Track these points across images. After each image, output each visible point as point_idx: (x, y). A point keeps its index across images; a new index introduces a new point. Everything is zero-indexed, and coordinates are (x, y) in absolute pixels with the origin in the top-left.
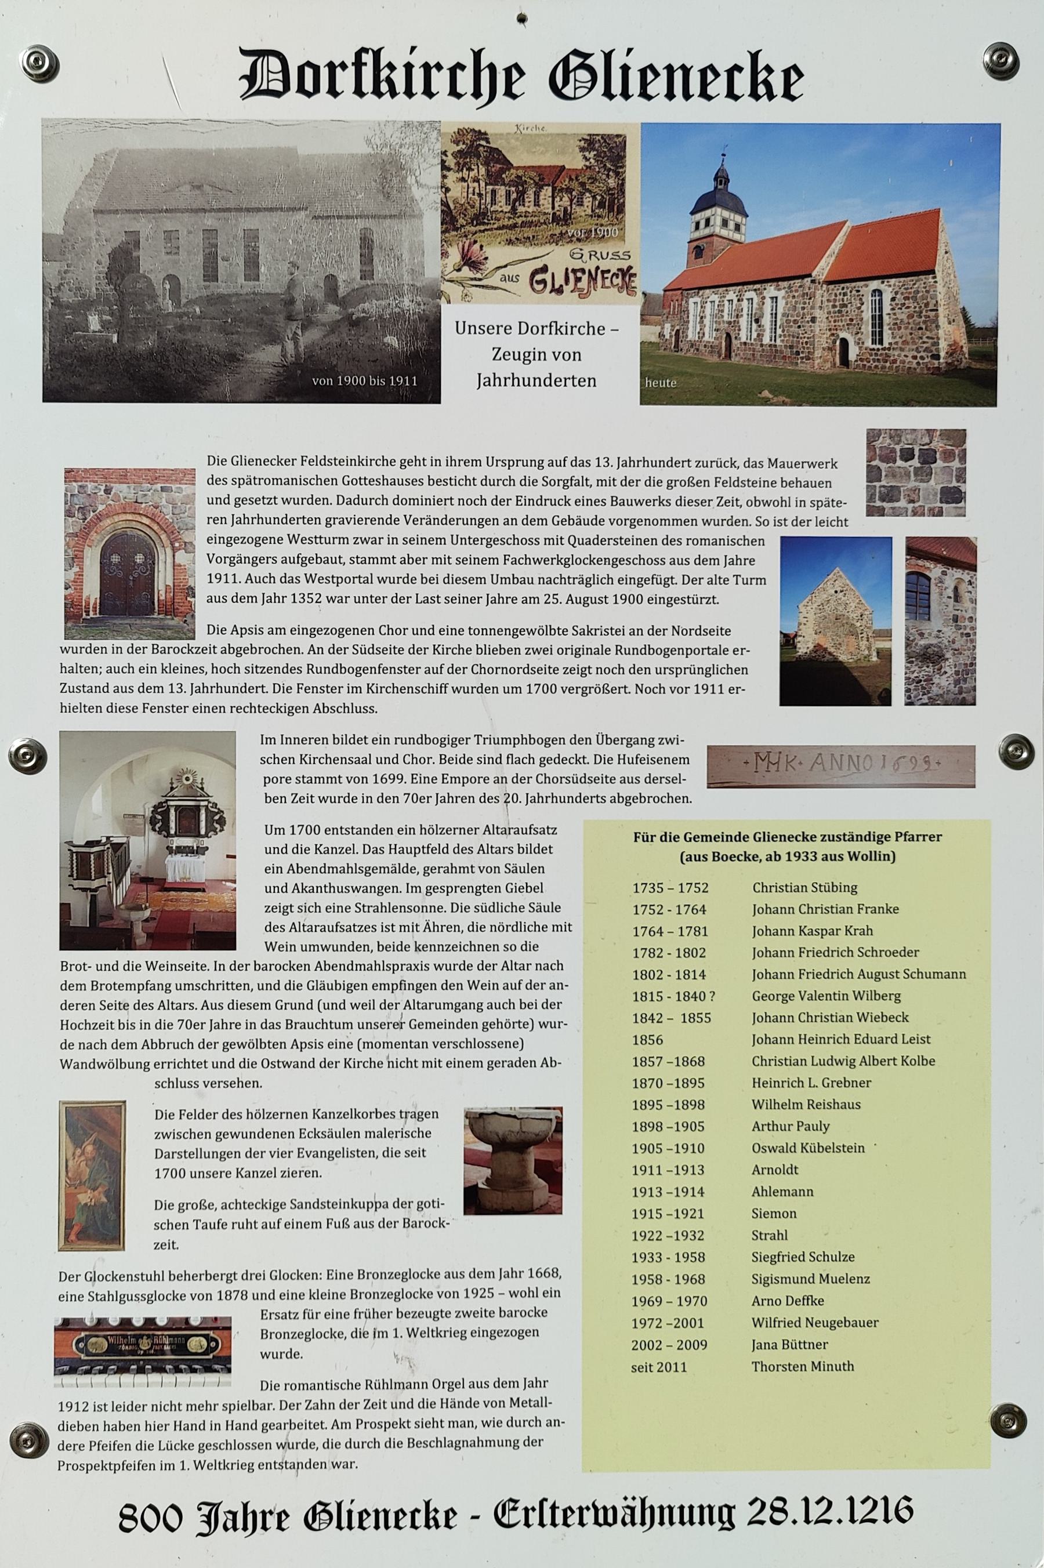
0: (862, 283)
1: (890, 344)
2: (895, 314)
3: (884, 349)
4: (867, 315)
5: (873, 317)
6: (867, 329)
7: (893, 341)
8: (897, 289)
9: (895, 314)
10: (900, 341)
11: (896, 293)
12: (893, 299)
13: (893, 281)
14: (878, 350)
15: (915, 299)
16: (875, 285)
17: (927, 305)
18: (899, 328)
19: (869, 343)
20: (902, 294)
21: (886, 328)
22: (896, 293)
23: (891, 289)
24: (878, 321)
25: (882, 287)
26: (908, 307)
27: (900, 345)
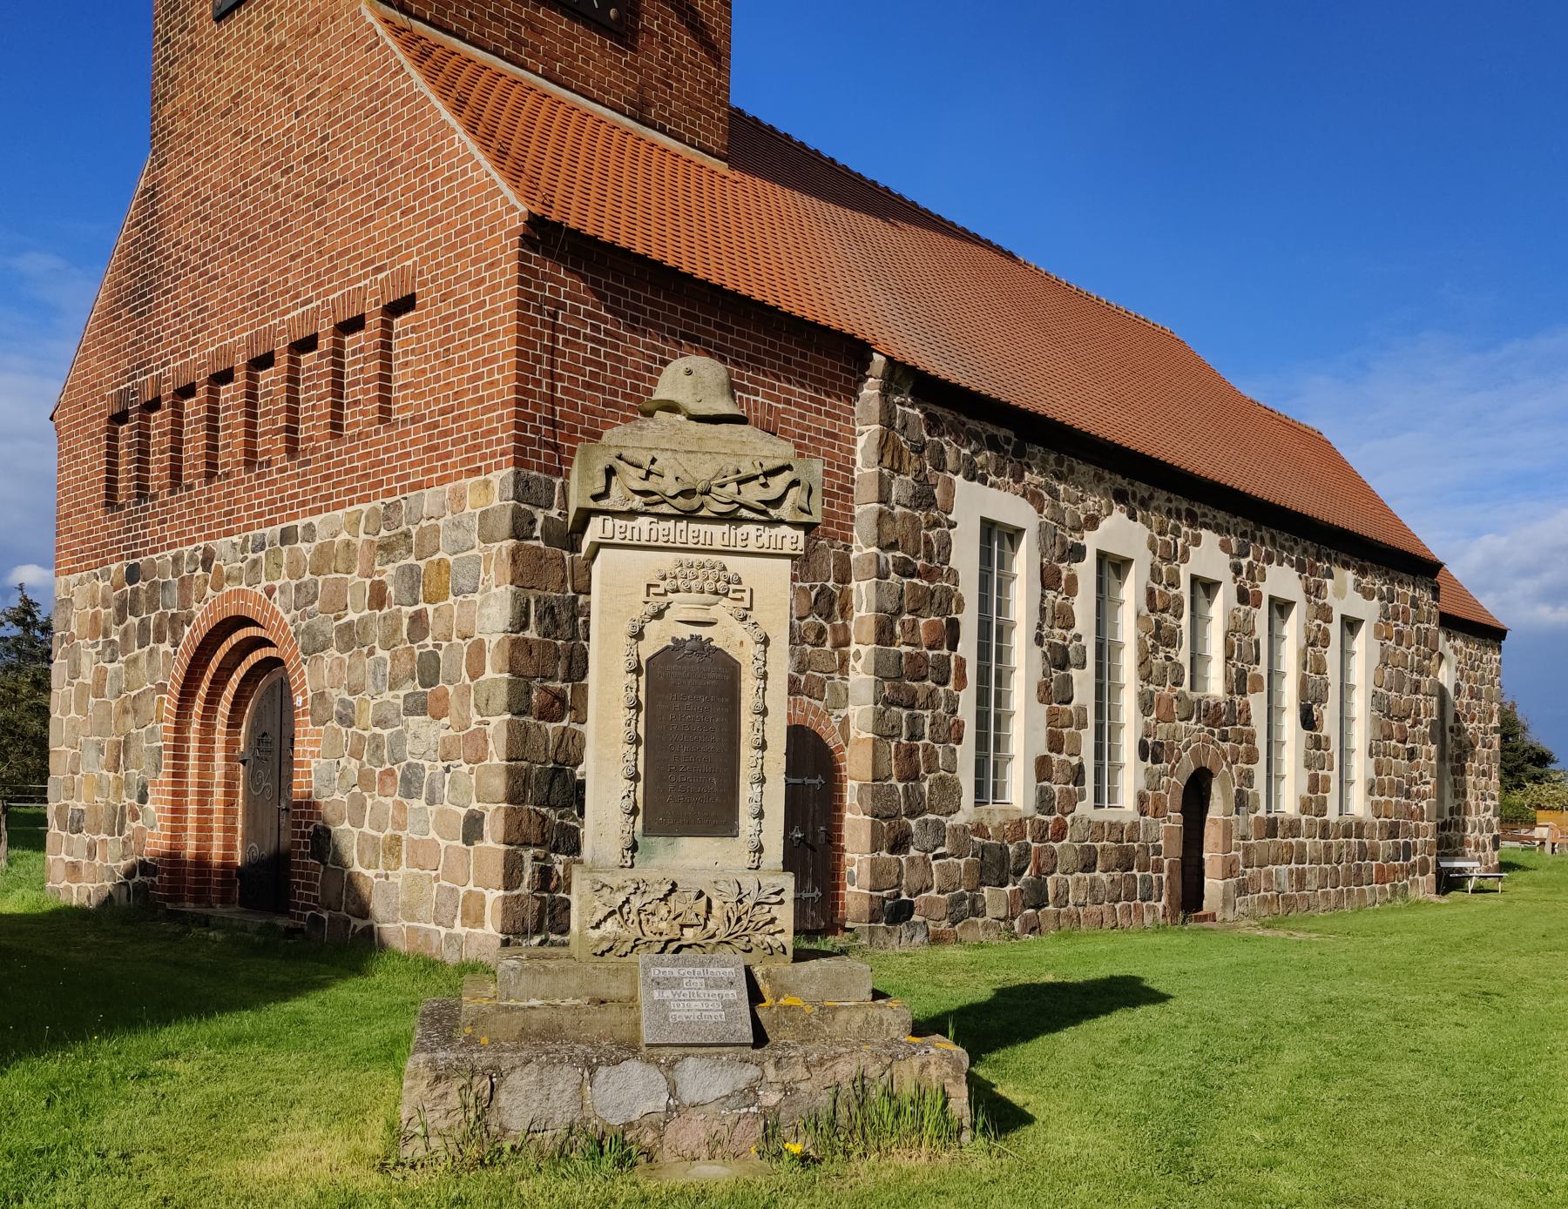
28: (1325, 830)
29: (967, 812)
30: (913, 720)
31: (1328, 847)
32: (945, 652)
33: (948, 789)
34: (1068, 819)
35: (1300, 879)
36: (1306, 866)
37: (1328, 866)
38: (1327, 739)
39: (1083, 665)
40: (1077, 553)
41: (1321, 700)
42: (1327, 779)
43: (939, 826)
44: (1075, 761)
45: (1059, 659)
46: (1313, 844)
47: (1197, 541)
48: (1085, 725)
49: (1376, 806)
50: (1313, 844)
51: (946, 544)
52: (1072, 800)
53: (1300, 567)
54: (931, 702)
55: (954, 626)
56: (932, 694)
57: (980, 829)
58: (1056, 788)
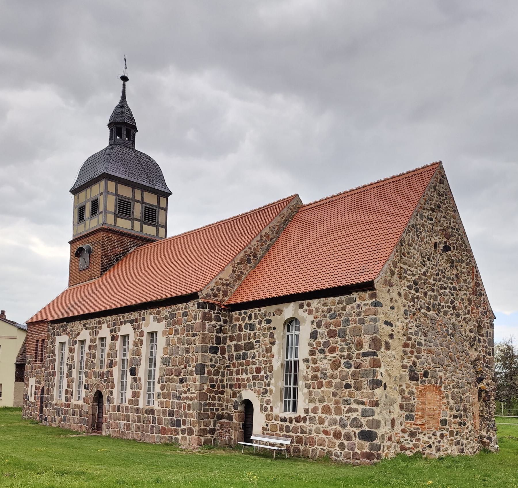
0: (272, 308)
3: (298, 420)
4: (277, 363)
6: (277, 384)
7: (311, 406)
9: (315, 362)
11: (319, 325)
12: (314, 336)
13: (315, 303)
15: (342, 334)
16: (289, 310)
17: (359, 345)
18: (320, 386)
20: (328, 325)
21: (301, 383)
22: (319, 325)
23: (311, 318)
26: (333, 350)
28: (137, 411)
31: (139, 417)
35: (127, 427)
37: (139, 424)
38: (140, 379)
39: (74, 368)
41: (138, 364)
42: (139, 393)
45: (71, 367)
46: (133, 415)
47: (101, 328)
49: (161, 404)
50: (133, 415)
53: (132, 321)
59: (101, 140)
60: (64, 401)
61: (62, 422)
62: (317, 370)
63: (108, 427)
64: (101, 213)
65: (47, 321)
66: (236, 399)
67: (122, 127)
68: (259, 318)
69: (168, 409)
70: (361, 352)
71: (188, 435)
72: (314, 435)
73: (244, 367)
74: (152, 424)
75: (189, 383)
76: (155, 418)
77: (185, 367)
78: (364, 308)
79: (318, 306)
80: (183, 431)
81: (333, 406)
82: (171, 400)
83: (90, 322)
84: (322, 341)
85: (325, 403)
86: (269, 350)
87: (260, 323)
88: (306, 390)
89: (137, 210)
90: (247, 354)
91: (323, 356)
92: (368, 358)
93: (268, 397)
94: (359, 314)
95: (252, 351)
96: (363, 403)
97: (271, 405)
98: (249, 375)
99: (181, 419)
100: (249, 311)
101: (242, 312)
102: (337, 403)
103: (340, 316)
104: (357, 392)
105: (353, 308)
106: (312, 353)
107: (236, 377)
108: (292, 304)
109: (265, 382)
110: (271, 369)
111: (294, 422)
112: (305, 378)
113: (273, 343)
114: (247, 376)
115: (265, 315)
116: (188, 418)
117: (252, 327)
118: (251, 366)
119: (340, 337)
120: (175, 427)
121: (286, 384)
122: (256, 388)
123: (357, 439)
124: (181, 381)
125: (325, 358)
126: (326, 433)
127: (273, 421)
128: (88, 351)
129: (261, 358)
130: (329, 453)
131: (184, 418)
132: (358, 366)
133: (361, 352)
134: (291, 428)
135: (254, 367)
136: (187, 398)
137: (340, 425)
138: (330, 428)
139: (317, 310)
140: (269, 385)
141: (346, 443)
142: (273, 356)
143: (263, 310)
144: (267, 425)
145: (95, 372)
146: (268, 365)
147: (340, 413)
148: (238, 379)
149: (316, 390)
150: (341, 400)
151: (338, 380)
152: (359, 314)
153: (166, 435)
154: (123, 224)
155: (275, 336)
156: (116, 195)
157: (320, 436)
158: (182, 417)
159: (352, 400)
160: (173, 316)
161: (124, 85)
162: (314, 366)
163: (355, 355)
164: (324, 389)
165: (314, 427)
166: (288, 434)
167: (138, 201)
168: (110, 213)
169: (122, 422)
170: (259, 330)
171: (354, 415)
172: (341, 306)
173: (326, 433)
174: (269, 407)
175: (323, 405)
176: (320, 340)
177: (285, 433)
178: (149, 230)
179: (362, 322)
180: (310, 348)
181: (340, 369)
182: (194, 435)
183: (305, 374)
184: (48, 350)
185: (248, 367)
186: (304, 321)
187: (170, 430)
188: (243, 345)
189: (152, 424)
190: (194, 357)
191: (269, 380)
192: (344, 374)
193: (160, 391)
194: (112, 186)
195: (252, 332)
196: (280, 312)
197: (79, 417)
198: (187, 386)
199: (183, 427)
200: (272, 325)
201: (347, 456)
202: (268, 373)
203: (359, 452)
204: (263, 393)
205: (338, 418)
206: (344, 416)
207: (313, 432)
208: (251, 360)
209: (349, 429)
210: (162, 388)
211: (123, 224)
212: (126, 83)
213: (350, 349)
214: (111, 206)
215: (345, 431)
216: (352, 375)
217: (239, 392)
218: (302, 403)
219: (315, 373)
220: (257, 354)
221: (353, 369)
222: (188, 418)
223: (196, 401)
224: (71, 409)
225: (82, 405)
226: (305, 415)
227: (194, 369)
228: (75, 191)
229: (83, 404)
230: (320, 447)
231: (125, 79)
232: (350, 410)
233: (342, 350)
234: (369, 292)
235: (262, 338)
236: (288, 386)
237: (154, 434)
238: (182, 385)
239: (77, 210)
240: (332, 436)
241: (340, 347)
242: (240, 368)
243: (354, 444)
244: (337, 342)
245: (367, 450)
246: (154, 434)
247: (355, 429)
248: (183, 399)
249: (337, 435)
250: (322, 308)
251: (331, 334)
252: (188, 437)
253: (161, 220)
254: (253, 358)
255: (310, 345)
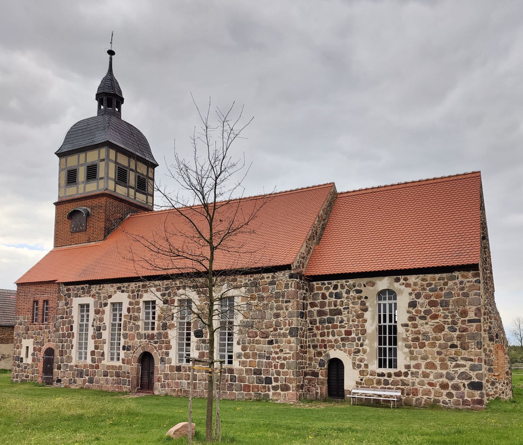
0: (364, 281)
1: (408, 367)
2: (415, 326)
3: (398, 374)
4: (371, 327)
5: (381, 330)
6: (371, 345)
7: (413, 363)
8: (418, 289)
9: (415, 326)
10: (423, 363)
11: (418, 296)
12: (412, 304)
13: (412, 279)
14: (390, 375)
15: (445, 304)
16: (383, 283)
17: (464, 313)
18: (422, 346)
19: (374, 366)
20: (427, 297)
21: (400, 343)
23: (409, 290)
24: (388, 335)
25: (397, 286)
26: (435, 317)
27: (423, 369)
29: (73, 363)
30: (63, 345)
32: (70, 332)
33: (70, 359)
34: (100, 364)
36: (197, 382)
39: (105, 330)
40: (106, 305)
43: (67, 365)
44: (102, 351)
45: (99, 329)
48: (105, 343)
49: (243, 363)
51: (71, 311)
52: (100, 360)
54: (66, 341)
55: (72, 327)
56: (67, 340)
57: (76, 366)
58: (97, 358)
59: (90, 109)
60: (89, 361)
61: (87, 384)
62: (418, 332)
63: (163, 386)
64: (101, 178)
65: (58, 283)
66: (322, 358)
67: (110, 97)
68: (346, 288)
69: (253, 368)
70: (467, 319)
71: (282, 390)
72: (417, 386)
73: (331, 330)
74: (229, 382)
75: (281, 345)
76: (235, 377)
77: (276, 330)
78: (468, 285)
79: (416, 281)
80: (275, 388)
81: (437, 363)
82: (257, 360)
83: (129, 285)
84: (423, 309)
85: (429, 360)
86: (359, 316)
87: (348, 292)
88: (407, 350)
89: (132, 179)
90: (333, 319)
91: (424, 321)
92: (475, 325)
93: (360, 355)
94: (462, 289)
95: (340, 316)
96: (471, 360)
97: (366, 362)
98: (336, 337)
99: (273, 377)
100: (334, 282)
101: (326, 282)
102: (442, 360)
103: (441, 289)
104: (463, 351)
105: (455, 284)
106: (412, 319)
107: (320, 338)
108: (386, 278)
109: (357, 343)
110: (364, 332)
111: (393, 377)
112: (405, 340)
113: (366, 310)
114: (334, 338)
115: (354, 286)
116: (282, 376)
117: (338, 296)
118: (339, 329)
119: (442, 306)
120: (264, 385)
121: (380, 344)
122: (346, 348)
123: (467, 389)
124: (271, 342)
125: (427, 324)
126: (431, 384)
127: (369, 376)
128: (127, 314)
129: (351, 323)
130: (436, 401)
131: (275, 376)
132: (465, 330)
133: (467, 319)
134: (390, 382)
135: (343, 330)
136: (279, 358)
137: (447, 378)
138: (436, 380)
139: (415, 284)
140: (362, 345)
141: (454, 392)
142: (366, 321)
143: (351, 282)
144: (362, 380)
145: (138, 334)
146: (360, 328)
147: (447, 368)
148: (323, 341)
149: (418, 349)
150: (447, 358)
151: (442, 342)
152: (462, 289)
153: (251, 392)
154: (121, 191)
155: (367, 304)
156: (116, 162)
157: (424, 387)
158: (273, 375)
159: (459, 358)
160: (255, 284)
161: (111, 59)
162: (414, 330)
163: (460, 322)
164: (427, 348)
165: (417, 380)
166: (387, 387)
167: (132, 170)
168: (111, 179)
169: (184, 381)
170: (347, 298)
171: (463, 370)
172: (442, 282)
173: (431, 384)
174: (362, 364)
175: (426, 362)
176: (420, 309)
177: (382, 386)
178: (141, 198)
179: (466, 295)
180: (409, 315)
181: (443, 333)
182: (291, 391)
183: (404, 336)
184: (61, 312)
185: (335, 330)
186: (401, 292)
187: (257, 387)
188: (328, 311)
189: (229, 382)
190: (287, 321)
191: (361, 341)
192: (449, 336)
193: (241, 351)
194: (112, 153)
195: (339, 300)
196: (373, 284)
197: (115, 378)
198: (279, 347)
199: (274, 384)
200: (363, 295)
201: (457, 403)
202: (360, 335)
203: (470, 399)
204: (355, 353)
205: (444, 372)
206: (451, 371)
207: (416, 384)
208: (339, 324)
209: (456, 381)
210: (244, 349)
211: (121, 191)
212: (113, 57)
213: (453, 316)
214: (112, 174)
215: (452, 383)
216: (457, 337)
217: (325, 352)
218: (402, 359)
219: (415, 336)
220: (345, 319)
221: (458, 333)
222: (282, 376)
223: (291, 360)
224: (101, 369)
225: (120, 367)
226: (406, 370)
227: (288, 332)
228: (60, 154)
229: (122, 364)
230: (425, 397)
231: (111, 53)
232: (457, 366)
233: (446, 317)
234: (472, 272)
235: (351, 305)
236: (383, 346)
237: (234, 391)
238: (271, 346)
239: (64, 174)
240: (438, 387)
241: (443, 315)
242: (326, 331)
243: (463, 393)
244: (440, 311)
245: (477, 397)
246: (234, 391)
247: (464, 381)
248: (274, 359)
249: (444, 386)
250: (420, 282)
251: (432, 304)
252: (282, 393)
253: (150, 190)
254: (341, 322)
255: (408, 312)
